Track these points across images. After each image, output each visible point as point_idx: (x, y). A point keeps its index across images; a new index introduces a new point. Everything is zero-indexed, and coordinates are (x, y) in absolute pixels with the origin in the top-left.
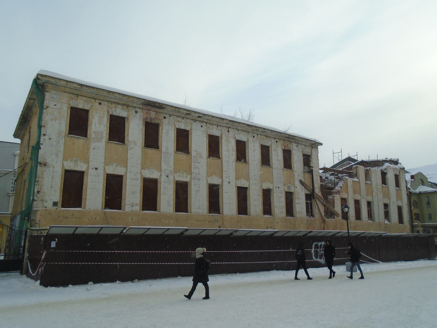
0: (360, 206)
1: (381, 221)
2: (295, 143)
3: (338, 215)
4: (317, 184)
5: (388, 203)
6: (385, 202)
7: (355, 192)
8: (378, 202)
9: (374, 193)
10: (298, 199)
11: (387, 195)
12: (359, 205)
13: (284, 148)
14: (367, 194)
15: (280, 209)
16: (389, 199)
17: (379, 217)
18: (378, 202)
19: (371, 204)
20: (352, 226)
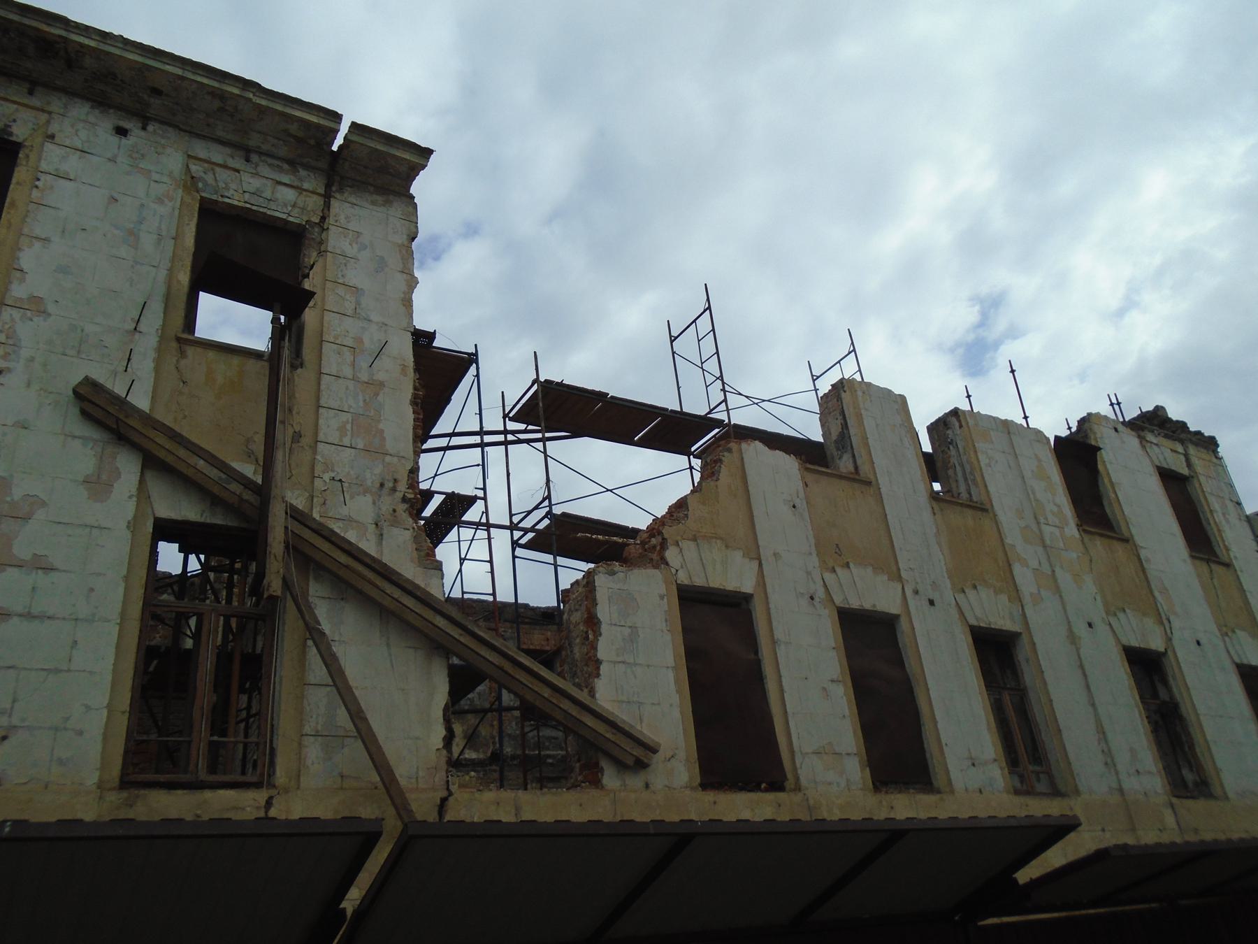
0: (910, 664)
1: (1131, 784)
2: (101, 102)
3: (636, 755)
4: (376, 451)
5: (1157, 644)
7: (833, 553)
8: (1073, 638)
9: (1017, 569)
11: (1138, 591)
12: (898, 660)
14: (964, 579)
16: (1162, 621)
17: (1108, 753)
18: (1073, 638)
19: (1022, 653)
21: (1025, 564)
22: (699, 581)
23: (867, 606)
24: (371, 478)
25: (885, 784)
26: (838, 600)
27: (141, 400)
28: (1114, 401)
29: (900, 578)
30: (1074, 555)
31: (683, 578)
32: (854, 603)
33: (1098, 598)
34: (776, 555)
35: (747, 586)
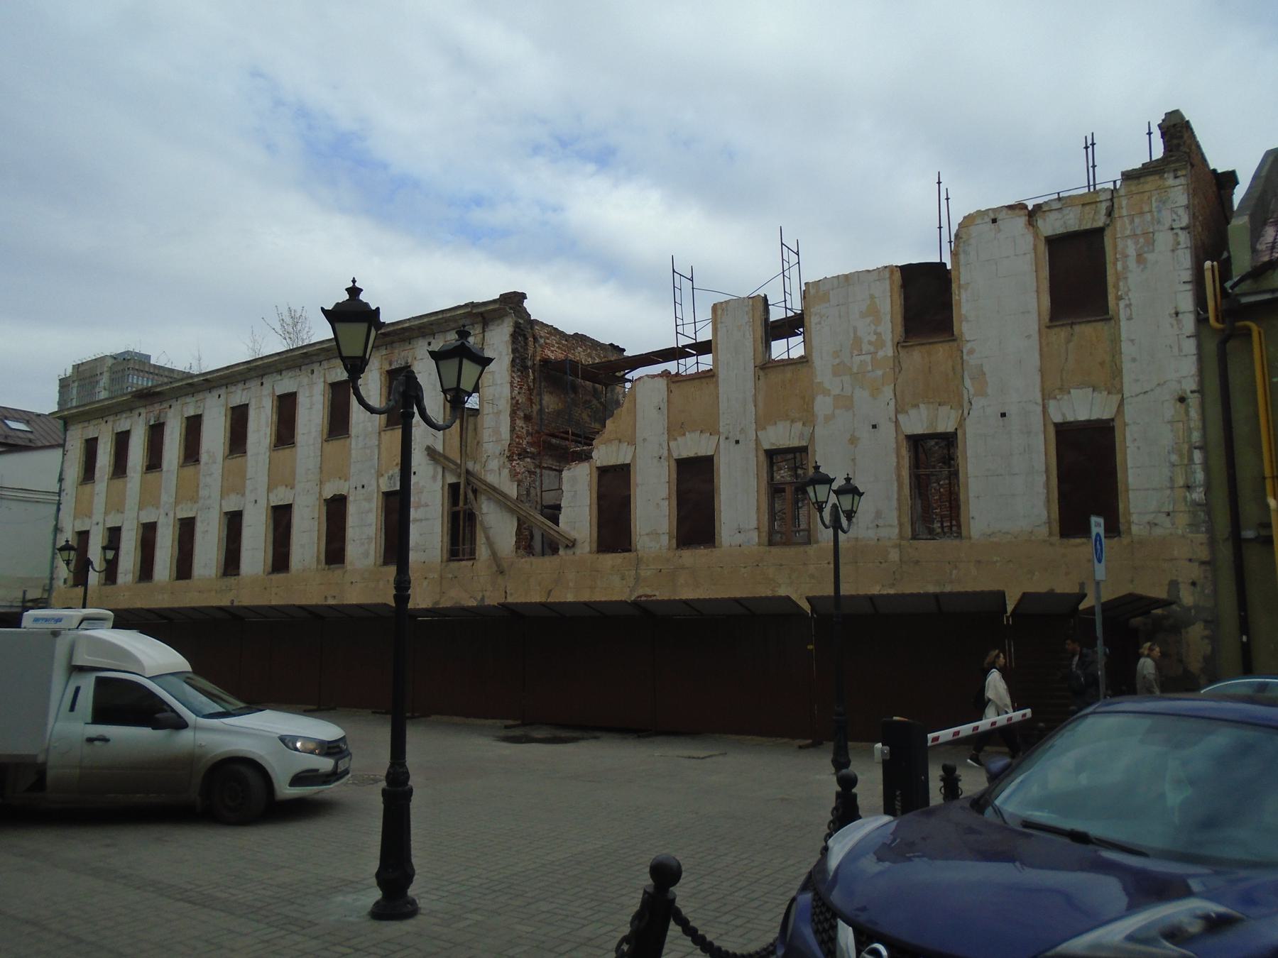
2: (424, 336)
6: (919, 430)
10: (417, 508)
13: (387, 367)
15: (363, 544)
18: (853, 441)
20: (644, 573)
21: (826, 392)
22: (605, 464)
23: (692, 454)
24: (497, 453)
25: (684, 545)
26: (676, 456)
27: (440, 448)
28: (1089, 142)
29: (719, 433)
30: (880, 373)
31: (599, 464)
32: (685, 454)
33: (892, 403)
34: (644, 440)
35: (627, 462)
